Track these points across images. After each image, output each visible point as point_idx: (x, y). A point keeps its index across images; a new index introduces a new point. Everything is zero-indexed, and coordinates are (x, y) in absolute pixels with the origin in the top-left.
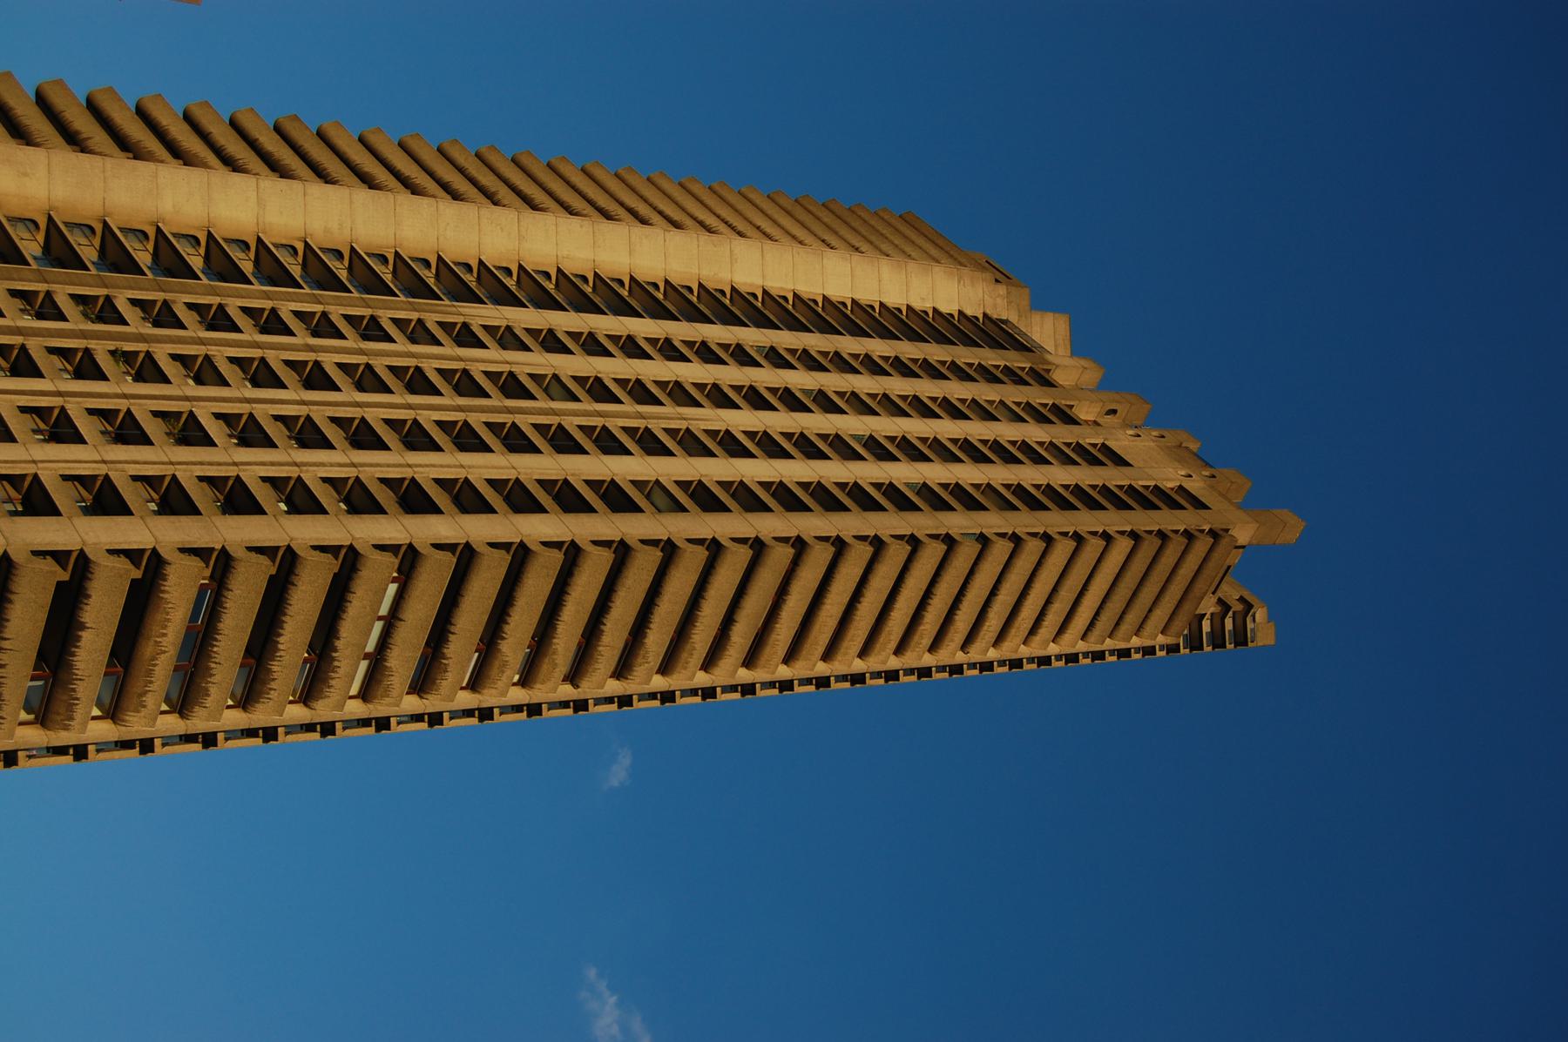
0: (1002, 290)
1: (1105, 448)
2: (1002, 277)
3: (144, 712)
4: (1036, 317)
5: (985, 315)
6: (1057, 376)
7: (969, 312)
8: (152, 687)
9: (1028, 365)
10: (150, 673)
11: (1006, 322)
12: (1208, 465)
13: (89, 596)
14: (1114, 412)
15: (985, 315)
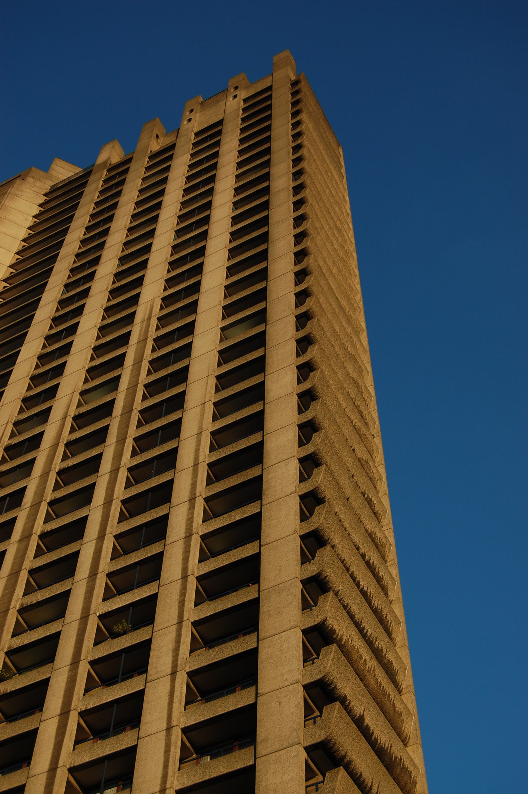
0: (30, 180)
1: (197, 134)
2: (22, 177)
3: (404, 715)
4: (53, 173)
5: (45, 195)
6: (115, 159)
7: (41, 201)
8: (392, 697)
9: (105, 172)
10: (384, 692)
11: (52, 187)
12: (225, 91)
13: (345, 697)
14: (157, 136)
15: (45, 195)
